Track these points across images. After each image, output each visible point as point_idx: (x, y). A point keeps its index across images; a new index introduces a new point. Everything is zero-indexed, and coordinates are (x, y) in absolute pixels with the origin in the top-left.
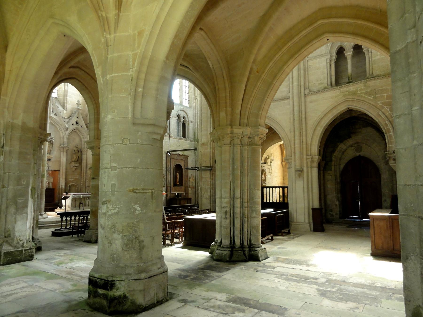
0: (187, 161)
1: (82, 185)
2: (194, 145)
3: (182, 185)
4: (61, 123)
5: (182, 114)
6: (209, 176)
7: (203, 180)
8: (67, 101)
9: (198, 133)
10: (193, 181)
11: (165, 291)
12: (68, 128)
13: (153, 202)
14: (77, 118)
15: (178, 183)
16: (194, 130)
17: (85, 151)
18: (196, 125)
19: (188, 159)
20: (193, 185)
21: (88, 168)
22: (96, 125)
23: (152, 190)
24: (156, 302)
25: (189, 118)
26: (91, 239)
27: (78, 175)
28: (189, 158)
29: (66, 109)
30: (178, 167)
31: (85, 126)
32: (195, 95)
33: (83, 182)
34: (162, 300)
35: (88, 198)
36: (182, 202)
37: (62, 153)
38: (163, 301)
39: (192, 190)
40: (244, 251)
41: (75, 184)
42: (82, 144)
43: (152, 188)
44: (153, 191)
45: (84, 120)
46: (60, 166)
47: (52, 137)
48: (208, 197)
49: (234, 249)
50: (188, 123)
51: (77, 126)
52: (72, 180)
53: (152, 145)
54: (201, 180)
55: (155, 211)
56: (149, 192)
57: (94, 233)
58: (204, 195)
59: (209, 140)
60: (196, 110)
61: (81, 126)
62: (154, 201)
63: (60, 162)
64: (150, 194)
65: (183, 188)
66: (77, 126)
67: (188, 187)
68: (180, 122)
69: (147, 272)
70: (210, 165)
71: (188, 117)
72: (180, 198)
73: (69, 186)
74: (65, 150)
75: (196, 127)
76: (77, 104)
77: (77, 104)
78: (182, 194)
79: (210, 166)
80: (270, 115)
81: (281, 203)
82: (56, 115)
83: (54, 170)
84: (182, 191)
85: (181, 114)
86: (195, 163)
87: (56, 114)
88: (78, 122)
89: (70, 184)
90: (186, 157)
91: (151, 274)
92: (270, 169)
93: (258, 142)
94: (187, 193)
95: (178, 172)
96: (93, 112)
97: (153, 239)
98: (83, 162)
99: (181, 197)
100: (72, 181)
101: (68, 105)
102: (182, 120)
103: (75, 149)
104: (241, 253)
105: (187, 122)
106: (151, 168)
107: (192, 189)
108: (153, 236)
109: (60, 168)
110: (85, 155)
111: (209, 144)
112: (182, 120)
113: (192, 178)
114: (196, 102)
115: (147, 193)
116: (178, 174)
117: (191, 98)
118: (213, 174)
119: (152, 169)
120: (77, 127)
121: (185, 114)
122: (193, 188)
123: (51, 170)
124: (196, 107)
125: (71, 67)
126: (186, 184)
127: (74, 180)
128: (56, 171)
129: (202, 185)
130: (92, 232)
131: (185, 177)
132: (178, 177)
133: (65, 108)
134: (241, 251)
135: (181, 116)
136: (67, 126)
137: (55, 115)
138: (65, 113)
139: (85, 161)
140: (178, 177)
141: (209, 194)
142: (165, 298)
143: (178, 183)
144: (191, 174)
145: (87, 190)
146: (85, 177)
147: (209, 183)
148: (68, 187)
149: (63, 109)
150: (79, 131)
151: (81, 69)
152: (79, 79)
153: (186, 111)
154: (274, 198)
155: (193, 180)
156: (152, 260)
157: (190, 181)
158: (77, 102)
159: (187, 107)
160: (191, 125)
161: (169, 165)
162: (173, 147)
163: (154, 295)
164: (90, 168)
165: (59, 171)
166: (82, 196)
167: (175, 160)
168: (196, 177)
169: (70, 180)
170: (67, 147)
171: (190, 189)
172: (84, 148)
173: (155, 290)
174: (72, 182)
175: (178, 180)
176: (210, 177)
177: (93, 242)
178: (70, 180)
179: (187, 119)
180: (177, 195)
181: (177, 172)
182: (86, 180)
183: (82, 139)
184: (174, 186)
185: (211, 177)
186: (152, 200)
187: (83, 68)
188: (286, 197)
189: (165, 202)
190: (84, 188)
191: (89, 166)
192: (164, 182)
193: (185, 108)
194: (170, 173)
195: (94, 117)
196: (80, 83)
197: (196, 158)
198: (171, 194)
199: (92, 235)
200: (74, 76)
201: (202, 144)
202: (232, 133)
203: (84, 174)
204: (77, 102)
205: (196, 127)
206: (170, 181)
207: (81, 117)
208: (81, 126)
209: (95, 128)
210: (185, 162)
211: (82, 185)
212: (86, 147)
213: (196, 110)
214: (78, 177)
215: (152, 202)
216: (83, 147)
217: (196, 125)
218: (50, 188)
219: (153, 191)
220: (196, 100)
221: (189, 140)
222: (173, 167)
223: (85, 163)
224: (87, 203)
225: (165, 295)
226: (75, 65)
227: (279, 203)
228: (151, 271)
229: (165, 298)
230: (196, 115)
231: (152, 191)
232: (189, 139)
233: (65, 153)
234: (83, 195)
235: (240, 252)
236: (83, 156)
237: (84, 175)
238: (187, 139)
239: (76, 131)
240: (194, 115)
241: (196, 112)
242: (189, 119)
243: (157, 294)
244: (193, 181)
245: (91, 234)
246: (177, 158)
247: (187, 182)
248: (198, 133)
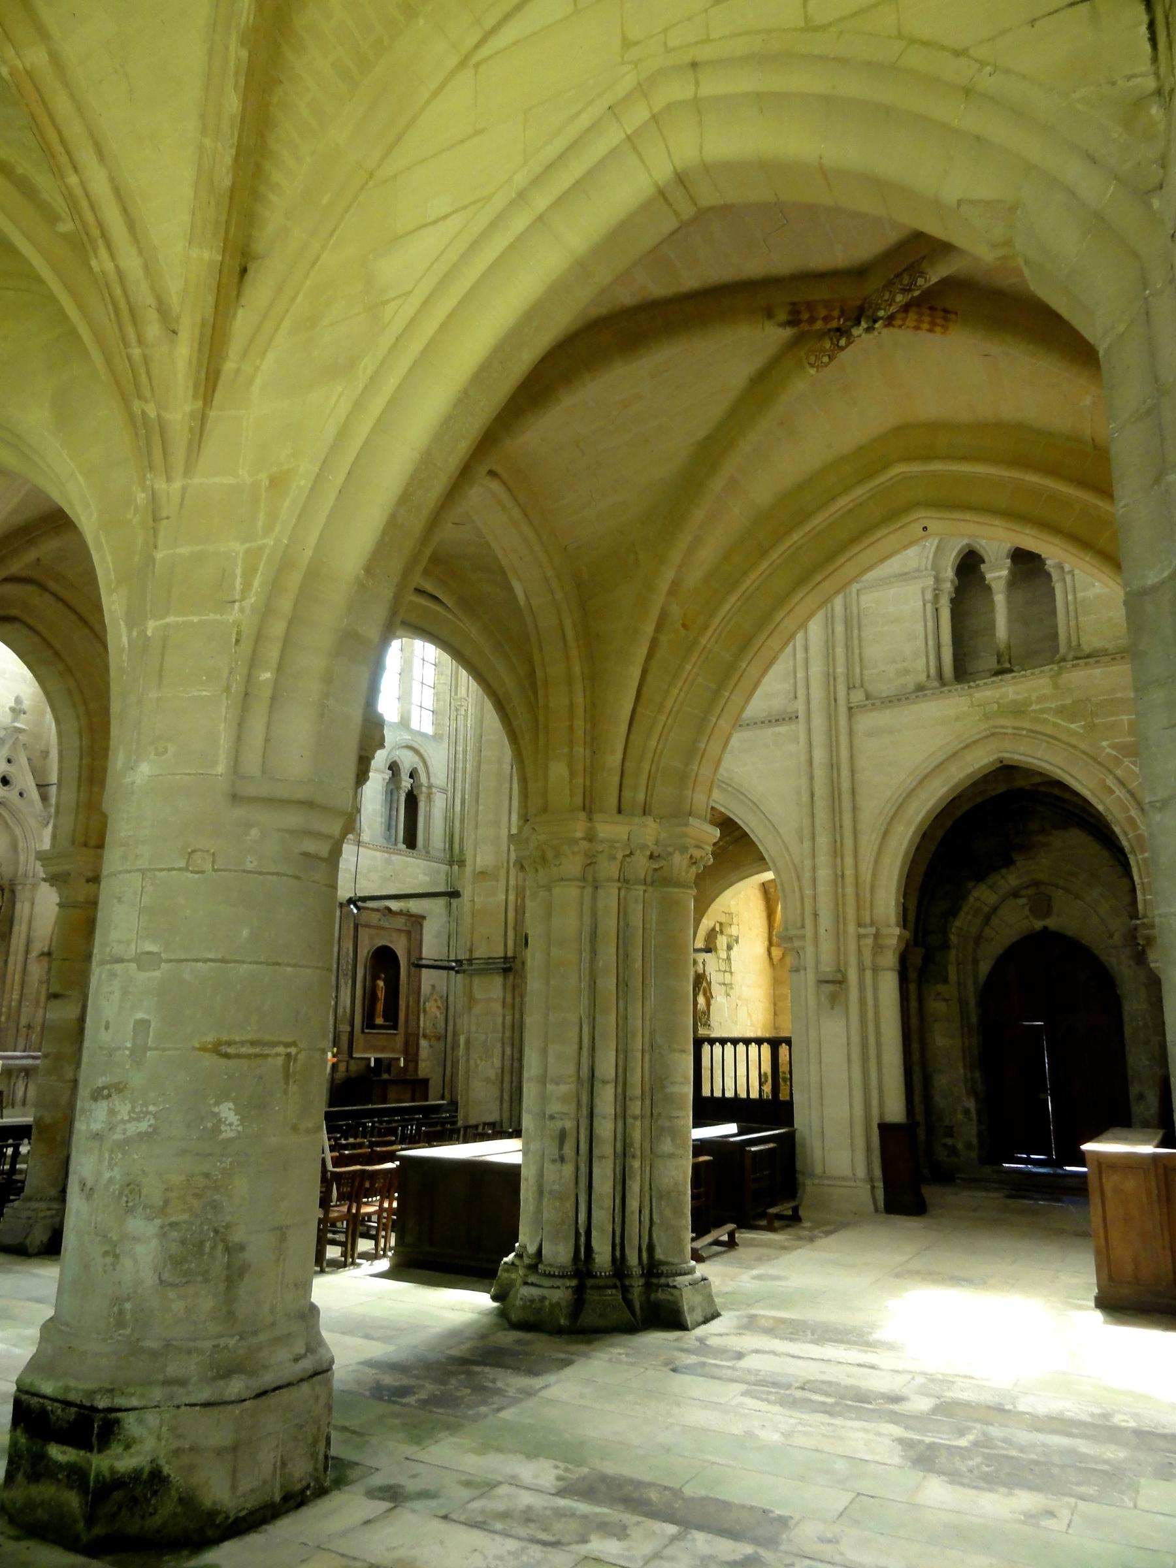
0: (418, 937)
2: (447, 875)
3: (395, 1027)
5: (407, 761)
6: (501, 995)
7: (477, 1010)
9: (462, 830)
10: (438, 1014)
11: (318, 1454)
13: (290, 1094)
14: (9, 761)
15: (379, 1021)
16: (449, 820)
18: (458, 802)
19: (421, 925)
20: (438, 1026)
21: (34, 954)
22: (82, 795)
23: (287, 1045)
24: (277, 1498)
25: (431, 775)
26: (26, 1238)
28: (426, 924)
30: (384, 959)
31: (34, 794)
32: (456, 694)
33: (10, 1008)
34: (303, 1491)
35: (23, 1074)
36: (392, 1092)
38: (308, 1493)
39: (431, 1046)
40: (625, 1290)
42: (17, 862)
43: (290, 1040)
44: (293, 1050)
45: (34, 771)
48: (492, 1074)
49: (590, 1282)
53: (298, 878)
54: (470, 1009)
55: (295, 1128)
56: (277, 1055)
57: (42, 1215)
58: (477, 1066)
59: (506, 858)
60: (460, 749)
62: (293, 1088)
64: (280, 1061)
65: (399, 1041)
67: (418, 1035)
68: (398, 788)
69: (252, 1374)
70: (506, 953)
71: (428, 773)
72: (385, 1076)
75: (458, 808)
76: (13, 710)
77: (13, 710)
78: (393, 1063)
79: (505, 958)
80: (725, 774)
81: (767, 1101)
84: (393, 1051)
86: (446, 943)
88: (8, 778)
90: (414, 919)
91: (268, 1379)
92: (725, 971)
93: (683, 874)
94: (412, 1056)
96: (77, 744)
97: (283, 1238)
98: (16, 929)
99: (389, 1072)
102: (406, 783)
104: (614, 1296)
105: (424, 789)
106: (289, 965)
107: (434, 1042)
108: (280, 1228)
110: (27, 905)
111: (503, 873)
112: (406, 783)
113: (436, 1001)
114: (461, 719)
115: (270, 1059)
116: (381, 983)
117: (442, 703)
118: (514, 987)
119: (295, 966)
120: (4, 797)
121: (416, 759)
122: (438, 1038)
124: (461, 737)
125: (8, 580)
126: (412, 1024)
129: (474, 1028)
130: (34, 1210)
131: (408, 997)
132: (381, 995)
134: (614, 1291)
135: (401, 767)
139: (24, 928)
140: (381, 995)
141: (497, 1062)
142: (317, 1480)
143: (379, 1021)
144: (433, 987)
145: (21, 1043)
146: (17, 987)
147: (500, 1020)
150: (12, 813)
151: (43, 587)
152: (30, 621)
153: (422, 751)
154: (742, 1081)
155: (438, 1007)
156: (273, 1324)
157: (425, 1011)
158: (13, 704)
159: (424, 735)
160: (439, 803)
161: (348, 950)
163: (275, 1465)
164: (43, 954)
167: (373, 932)
168: (451, 999)
171: (423, 1043)
172: (25, 875)
173: (277, 1446)
175: (380, 1006)
176: (504, 999)
177: (36, 1250)
179: (423, 779)
180: (372, 1064)
181: (379, 978)
182: (20, 1001)
183: (21, 844)
184: (363, 1032)
185: (509, 1000)
186: (287, 1083)
187: (52, 585)
188: (785, 1080)
190: (12, 1032)
191: (39, 946)
193: (419, 739)
195: (76, 762)
196: (37, 639)
197: (453, 925)
198: (352, 1062)
199: (31, 1222)
200: (14, 612)
201: (479, 872)
202: (590, 838)
203: (17, 978)
204: (13, 704)
205: (458, 808)
206: (348, 1011)
207: (22, 759)
208: (21, 794)
209: (78, 804)
210: (409, 939)
212: (31, 875)
213: (460, 749)
215: (286, 1092)
216: (20, 872)
217: (458, 802)
219: (293, 1050)
221: (428, 856)
222: (364, 960)
223: (23, 936)
224: (20, 1093)
225: (316, 1469)
226: (24, 574)
227: (760, 1101)
228: (265, 1367)
229: (317, 1480)
230: (460, 765)
231: (289, 1050)
232: (428, 852)
235: (611, 1295)
236: (18, 906)
238: (423, 852)
240: (452, 766)
241: (460, 756)
242: (433, 780)
243: (284, 1464)
244: (438, 1014)
245: (29, 1218)
246: (382, 923)
248: (462, 830)
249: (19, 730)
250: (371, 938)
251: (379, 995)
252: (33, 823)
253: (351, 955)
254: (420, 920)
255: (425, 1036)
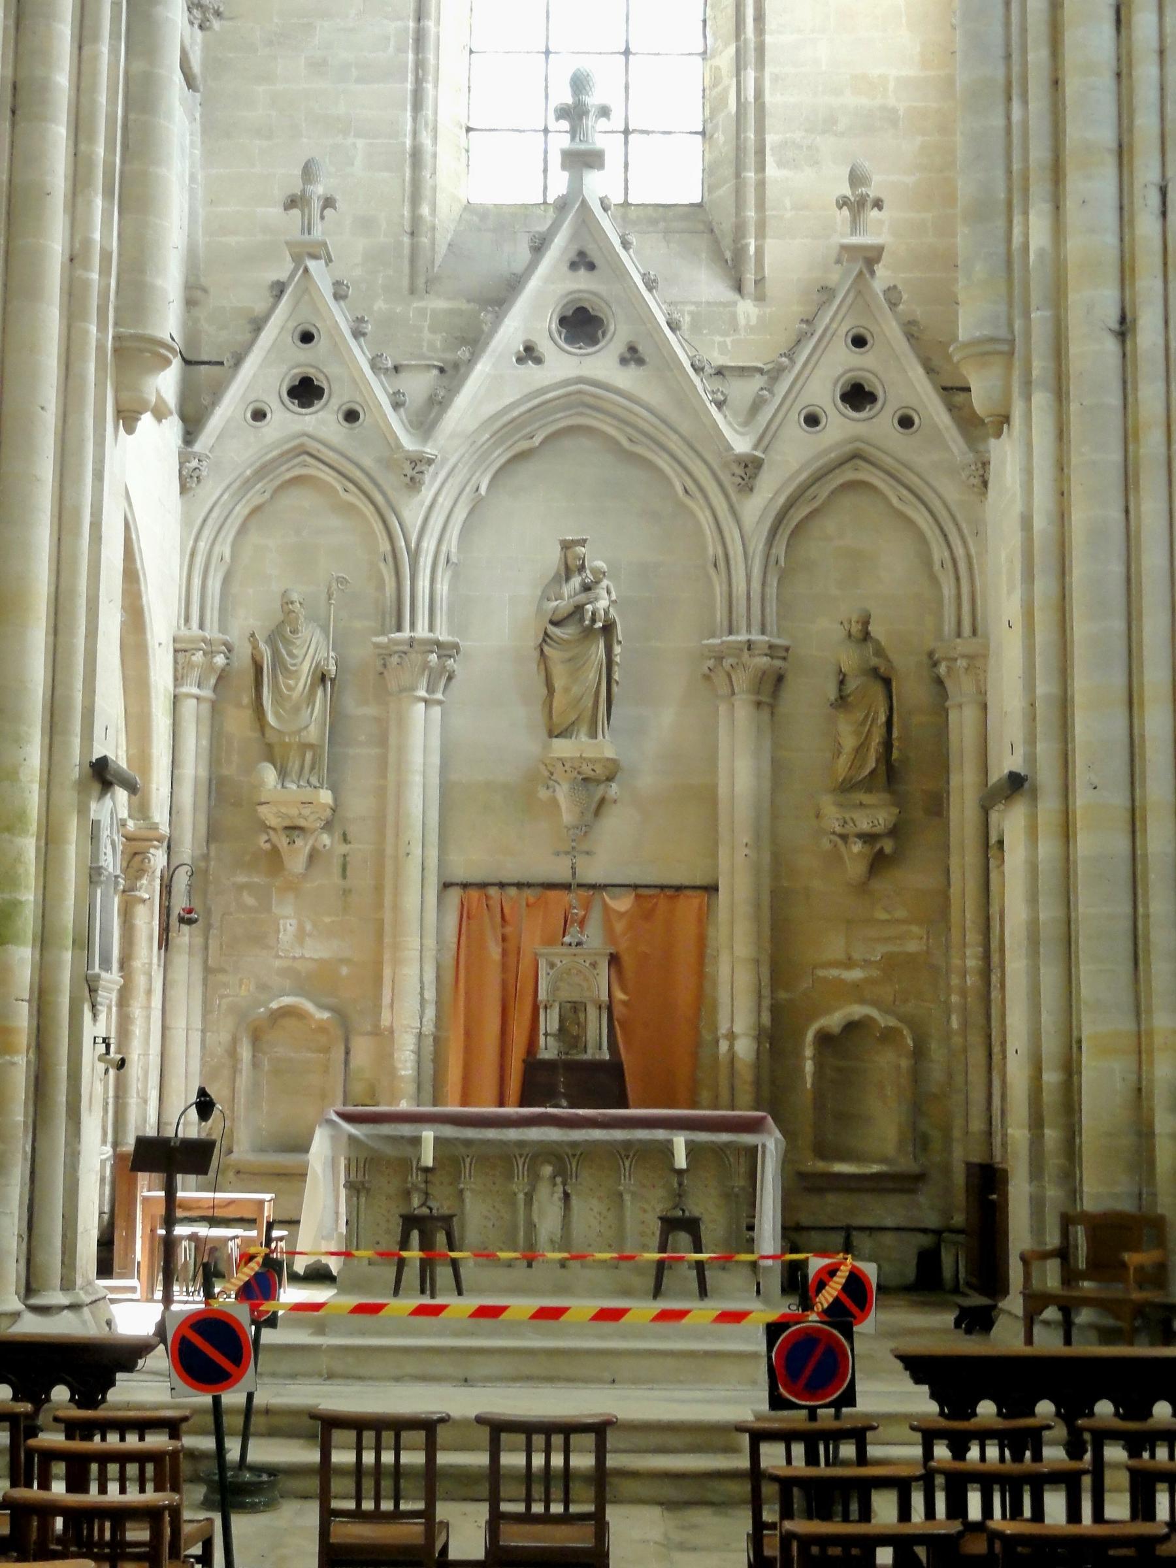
1: (955, 1024)
4: (685, 427)
8: (761, 205)
12: (750, 468)
17: (963, 663)
27: (915, 929)
29: (760, 282)
33: (963, 994)
35: (547, 1170)
37: (723, 708)
41: (884, 1020)
46: (714, 855)
47: (596, 572)
51: (861, 429)
52: (856, 974)
61: (906, 422)
63: (708, 798)
66: (861, 429)
73: (825, 1039)
74: (742, 681)
82: (640, 362)
83: (662, 887)
87: (640, 348)
89: (833, 1021)
100: (857, 986)
101: (772, 246)
103: (849, 659)
109: (715, 867)
123: (636, 887)
127: (875, 973)
128: (679, 888)
133: (750, 277)
136: (741, 445)
137: (632, 356)
138: (750, 329)
148: (809, 1052)
149: (731, 295)
165: (711, 889)
166: (437, 1140)
169: (834, 973)
170: (750, 645)
174: (856, 992)
178: (834, 973)
207: (889, 330)
208: (906, 422)
211: (955, 1024)
214: (912, 947)
218: (587, 1056)
233: (743, 711)
234: (449, 1131)
236: (953, 716)
237: (968, 924)
239: (860, 476)
249: (871, 258)
252: (952, 492)
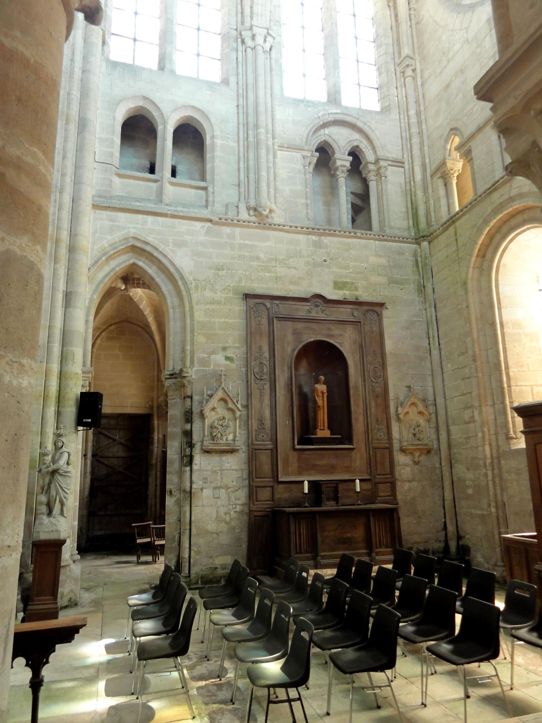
3: (349, 439)
10: (422, 421)
15: (324, 433)
19: (380, 316)
28: (386, 314)
50: (378, 174)
67: (390, 449)
71: (374, 148)
85: (336, 138)
90: (365, 308)
95: (322, 378)
99: (336, 499)
105: (371, 167)
117: (385, 74)
121: (356, 136)
135: (334, 146)
143: (324, 433)
153: (366, 128)
155: (420, 413)
157: (398, 419)
161: (260, 348)
162: (290, 268)
167: (300, 325)
171: (401, 459)
180: (306, 491)
181: (317, 381)
189: (246, 529)
192: (231, 429)
194: (267, 387)
206: (268, 423)
220: (409, 72)
244: (422, 421)
247: (383, 427)
250: (297, 334)
251: (320, 402)
253: (267, 355)
254: (377, 309)
255: (403, 450)
